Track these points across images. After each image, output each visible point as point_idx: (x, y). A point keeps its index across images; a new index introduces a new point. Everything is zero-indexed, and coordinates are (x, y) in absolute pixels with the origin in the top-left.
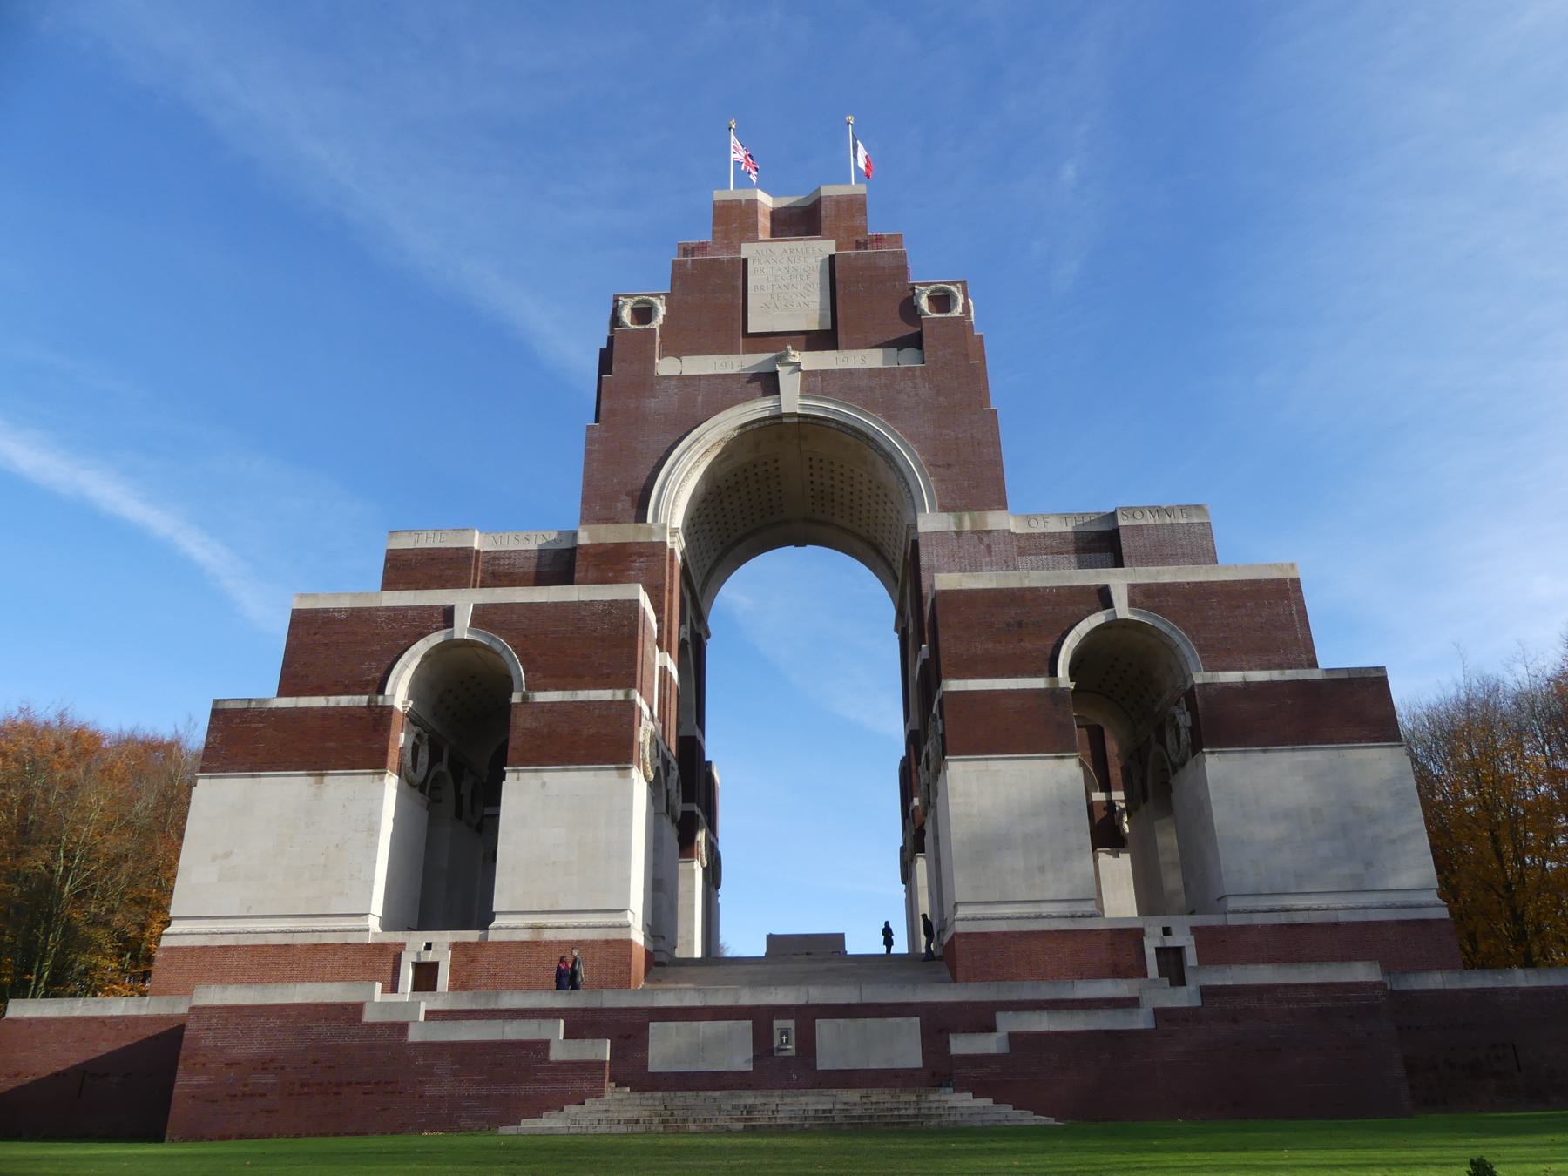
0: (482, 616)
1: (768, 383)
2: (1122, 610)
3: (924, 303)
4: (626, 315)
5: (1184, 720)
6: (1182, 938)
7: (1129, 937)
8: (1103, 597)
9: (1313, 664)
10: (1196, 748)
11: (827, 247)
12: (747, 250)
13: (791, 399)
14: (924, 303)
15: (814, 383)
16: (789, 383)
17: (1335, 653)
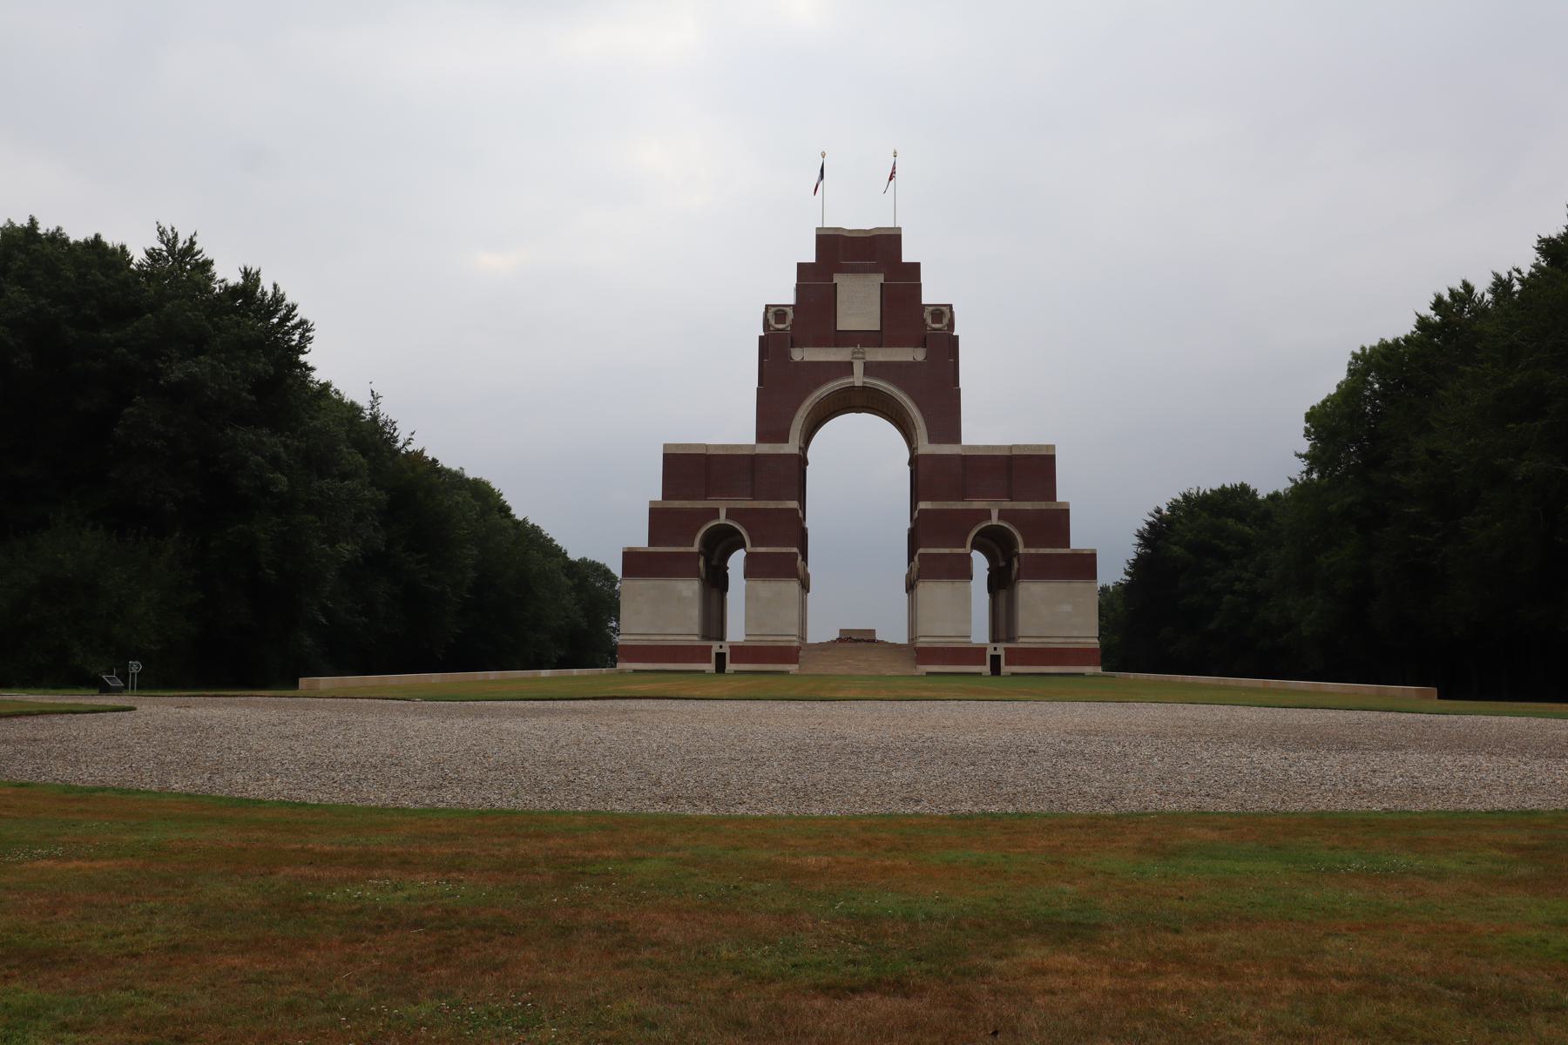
0: (731, 513)
1: (847, 368)
2: (995, 521)
3: (929, 320)
4: (772, 322)
5: (1016, 565)
6: (1001, 652)
7: (983, 650)
8: (986, 514)
9: (1067, 545)
10: (1018, 577)
11: (880, 278)
12: (838, 278)
13: (858, 379)
14: (929, 320)
15: (871, 369)
16: (858, 368)
17: (1079, 540)
